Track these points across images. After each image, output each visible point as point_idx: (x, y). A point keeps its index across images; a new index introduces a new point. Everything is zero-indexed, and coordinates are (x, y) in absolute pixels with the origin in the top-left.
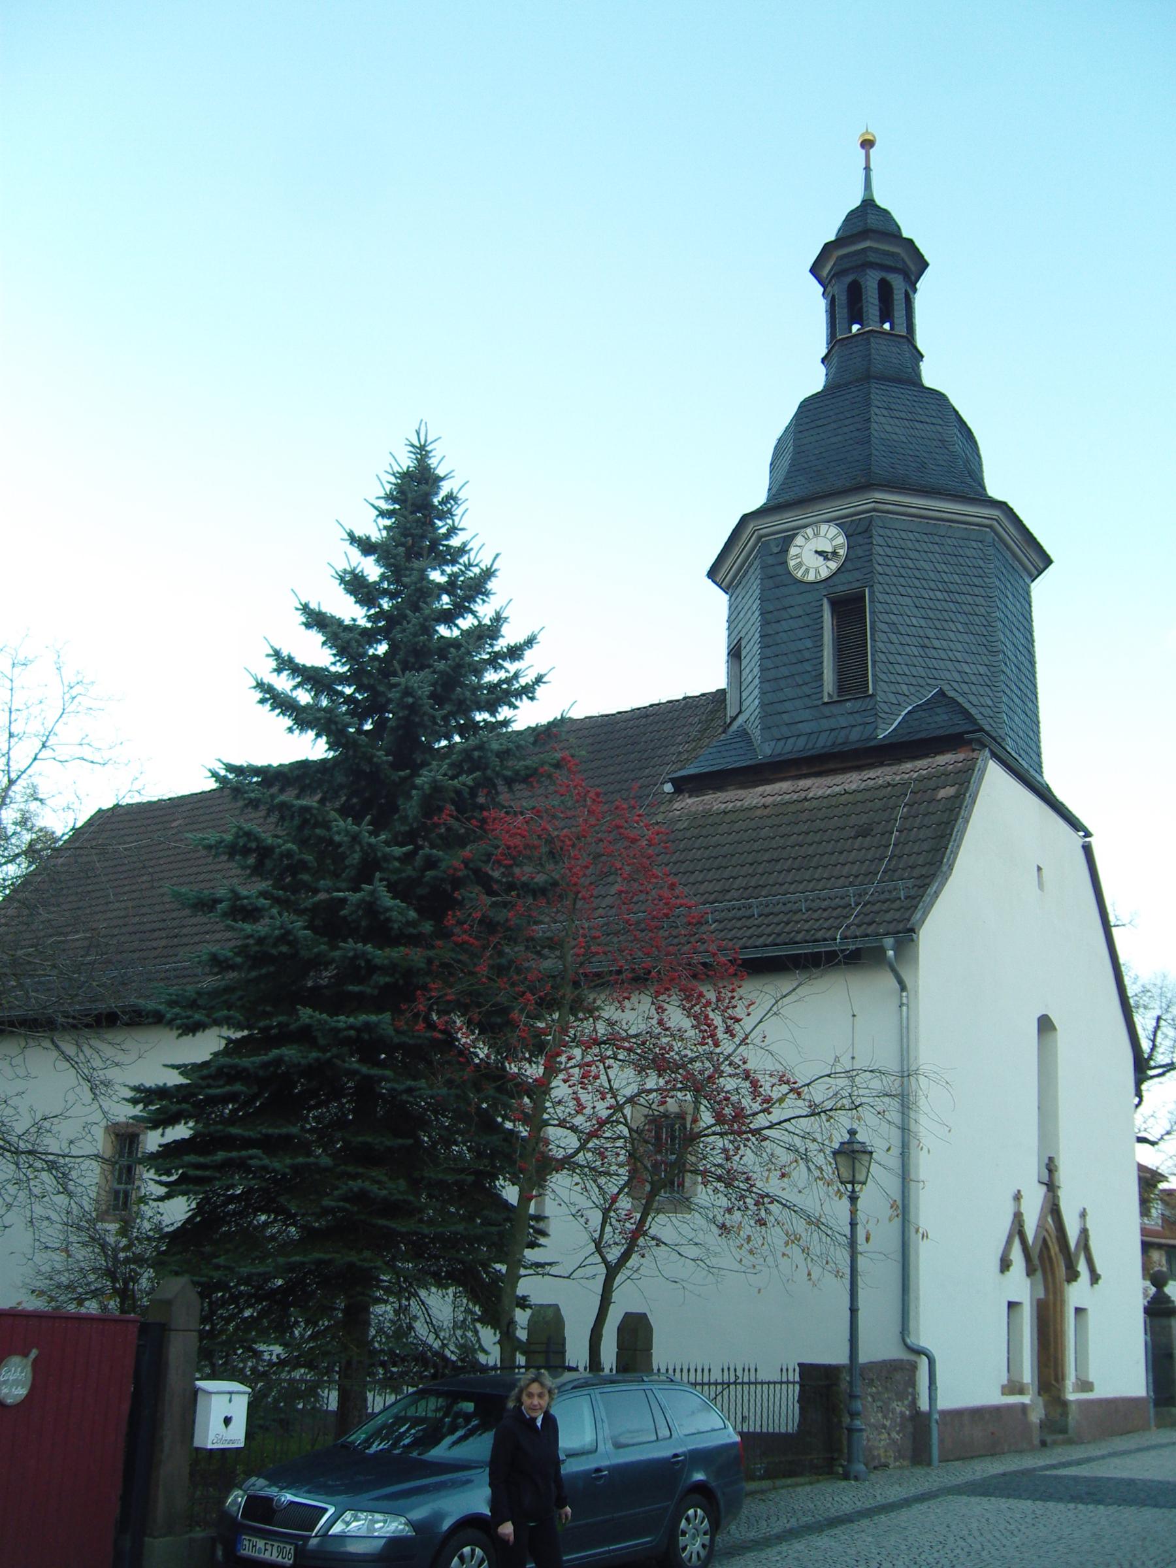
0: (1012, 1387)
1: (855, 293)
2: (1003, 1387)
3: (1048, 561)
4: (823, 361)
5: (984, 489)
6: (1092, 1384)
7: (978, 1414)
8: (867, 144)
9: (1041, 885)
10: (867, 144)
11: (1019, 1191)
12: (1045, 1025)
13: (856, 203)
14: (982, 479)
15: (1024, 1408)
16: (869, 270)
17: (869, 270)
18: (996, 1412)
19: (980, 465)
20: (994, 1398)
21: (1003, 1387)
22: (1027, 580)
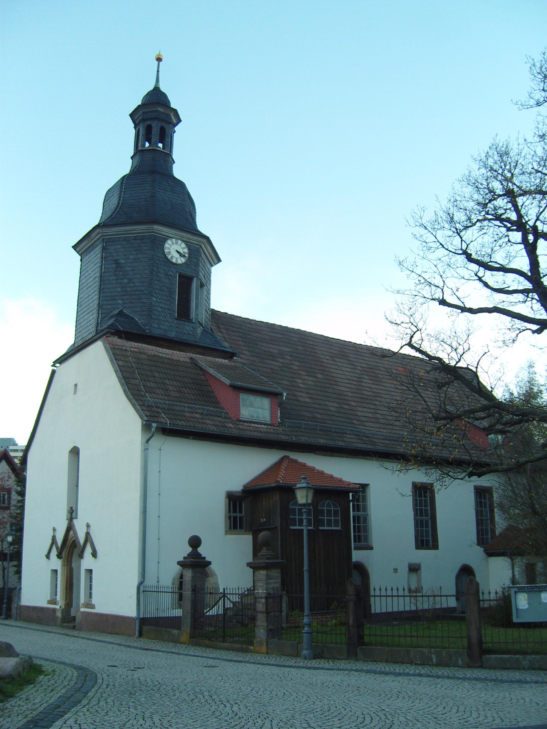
0: (53, 601)
1: (149, 130)
2: (48, 601)
3: (219, 260)
4: (132, 158)
5: (195, 222)
6: (94, 605)
7: (35, 608)
8: (159, 60)
9: (75, 392)
10: (159, 60)
11: (88, 523)
12: (75, 452)
13: (151, 88)
14: (195, 219)
15: (54, 610)
16: (155, 119)
17: (155, 119)
18: (42, 609)
19: (195, 213)
20: (45, 605)
21: (48, 601)
22: (209, 266)
